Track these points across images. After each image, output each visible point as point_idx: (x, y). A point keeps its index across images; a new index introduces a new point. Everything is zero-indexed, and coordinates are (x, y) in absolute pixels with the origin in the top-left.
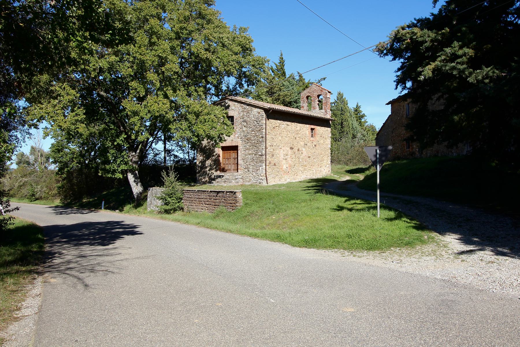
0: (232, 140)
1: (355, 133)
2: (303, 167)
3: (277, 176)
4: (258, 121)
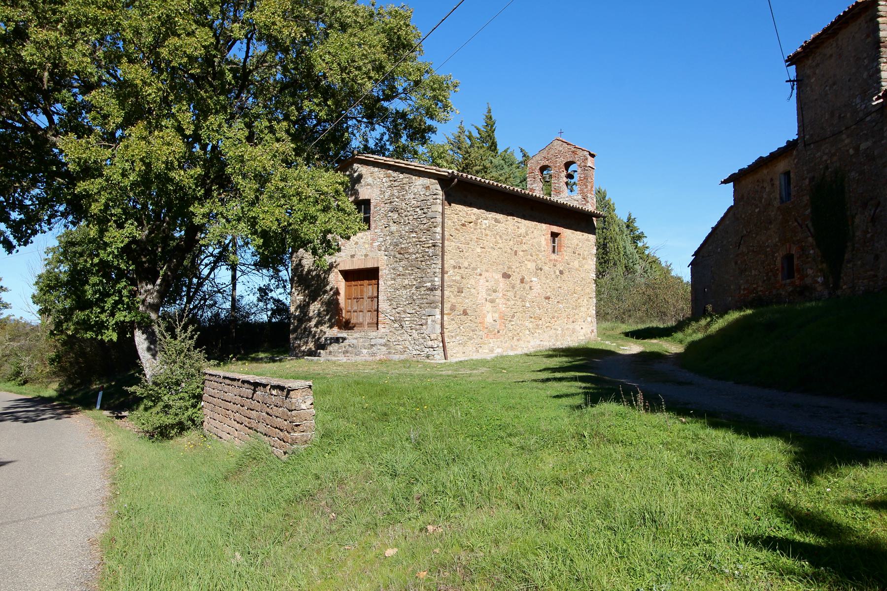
0: (366, 256)
1: (630, 264)
2: (532, 320)
3: (471, 340)
4: (424, 206)
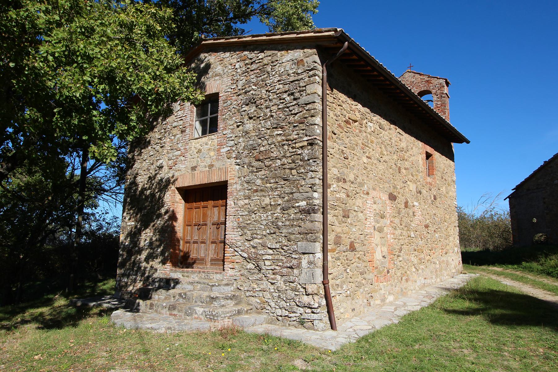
0: (211, 166)
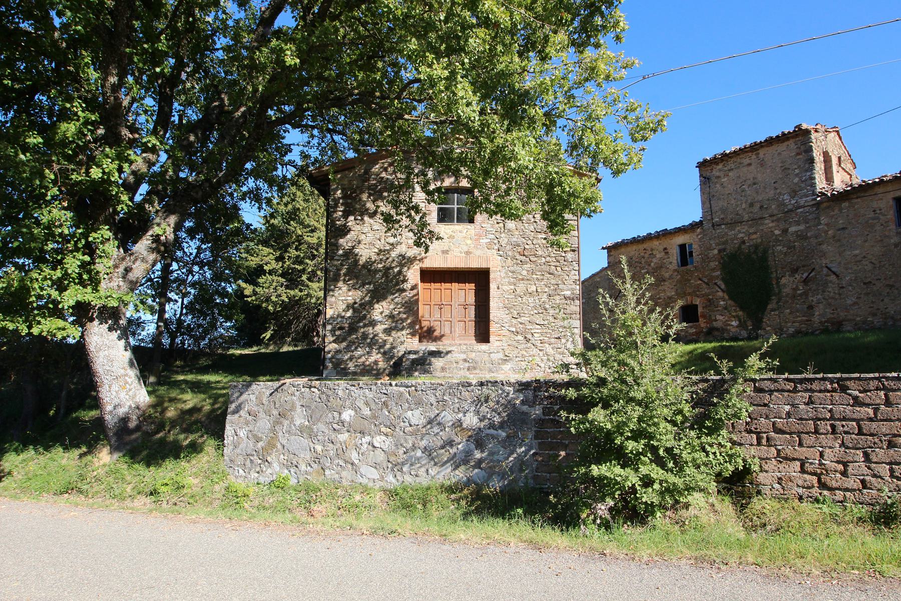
0: (468, 253)
